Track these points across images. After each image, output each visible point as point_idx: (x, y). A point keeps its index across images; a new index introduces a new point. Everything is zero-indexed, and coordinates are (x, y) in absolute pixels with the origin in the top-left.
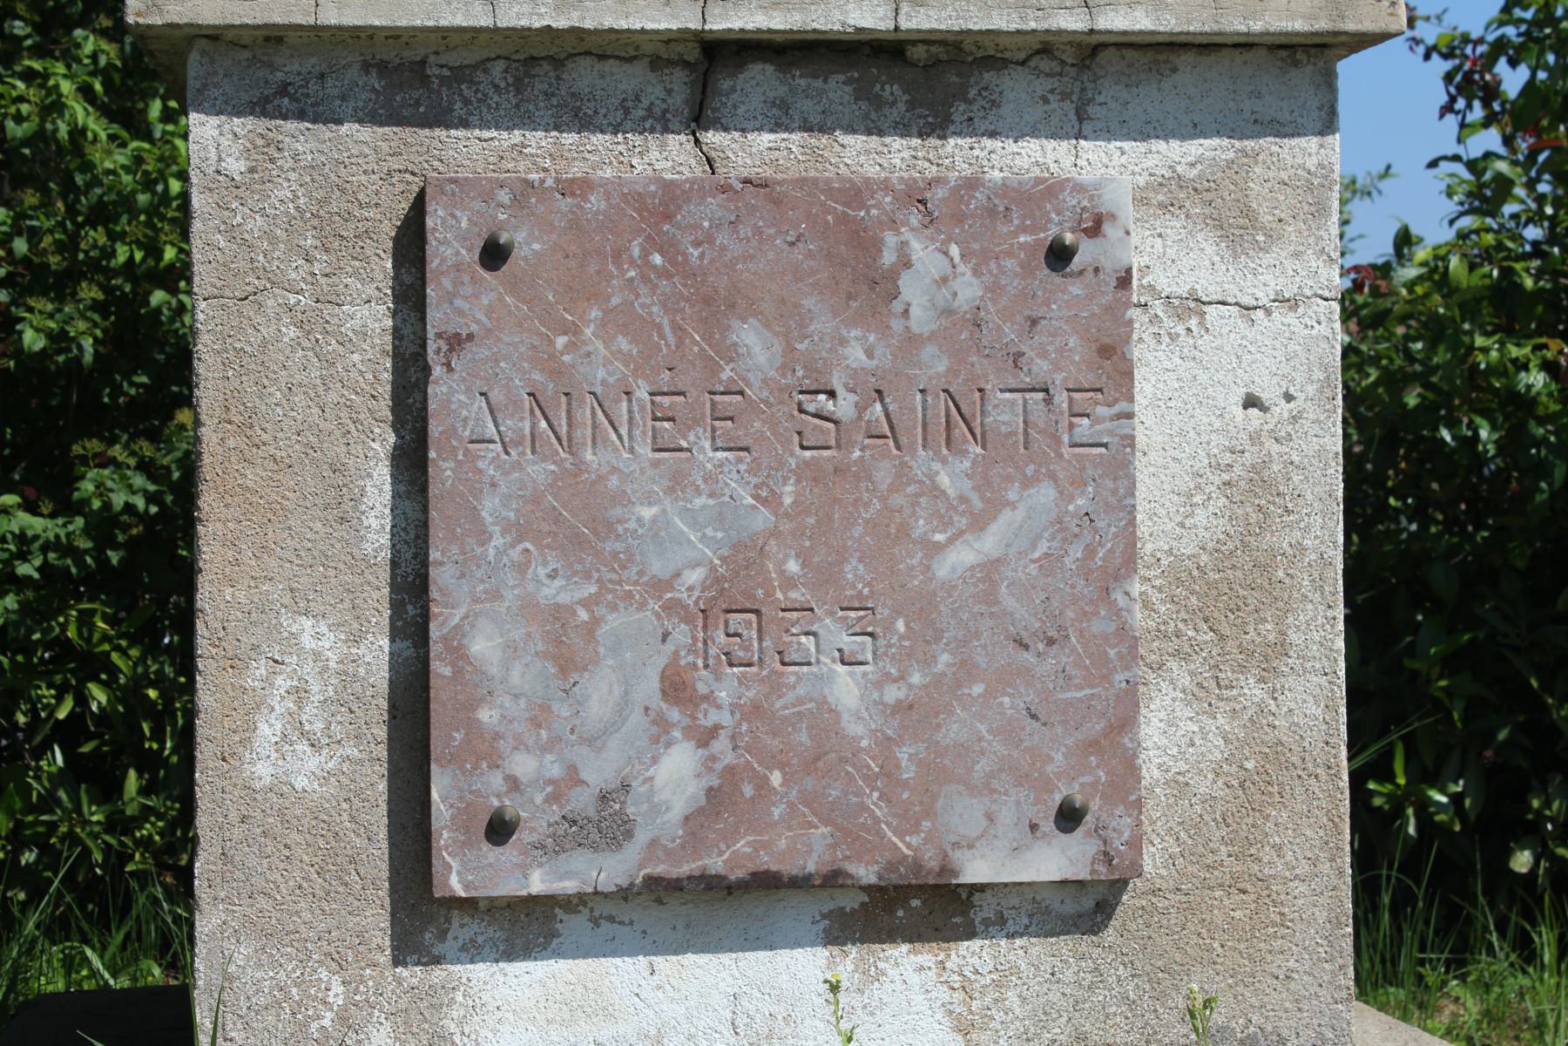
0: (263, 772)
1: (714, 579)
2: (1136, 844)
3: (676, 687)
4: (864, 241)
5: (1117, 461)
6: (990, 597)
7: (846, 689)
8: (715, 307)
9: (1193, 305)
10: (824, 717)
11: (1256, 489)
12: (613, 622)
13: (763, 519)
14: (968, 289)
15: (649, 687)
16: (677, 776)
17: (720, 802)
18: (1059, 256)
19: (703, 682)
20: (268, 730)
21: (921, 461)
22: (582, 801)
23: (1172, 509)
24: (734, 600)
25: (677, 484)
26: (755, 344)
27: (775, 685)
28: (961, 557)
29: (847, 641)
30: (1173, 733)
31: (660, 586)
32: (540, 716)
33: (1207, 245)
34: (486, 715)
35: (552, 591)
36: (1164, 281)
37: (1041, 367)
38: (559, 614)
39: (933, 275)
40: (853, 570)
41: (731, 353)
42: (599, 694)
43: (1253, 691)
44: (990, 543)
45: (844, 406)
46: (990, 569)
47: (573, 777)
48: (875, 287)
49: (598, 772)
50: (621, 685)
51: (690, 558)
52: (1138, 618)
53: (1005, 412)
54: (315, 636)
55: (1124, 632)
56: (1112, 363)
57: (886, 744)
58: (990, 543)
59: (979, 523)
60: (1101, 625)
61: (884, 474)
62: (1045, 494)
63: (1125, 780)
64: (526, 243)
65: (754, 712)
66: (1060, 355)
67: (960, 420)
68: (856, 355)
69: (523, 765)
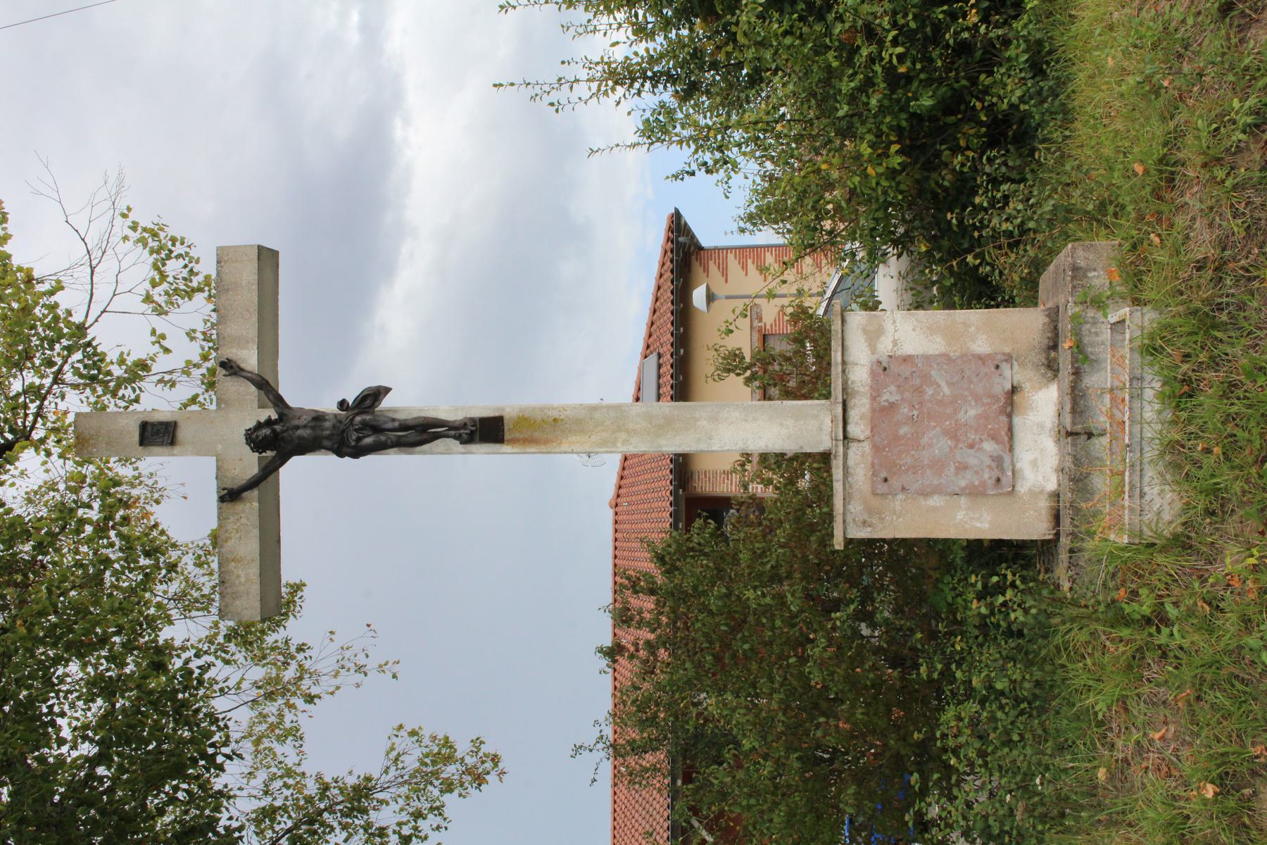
0: (986, 526)
1: (951, 438)
2: (1004, 354)
3: (971, 446)
4: (883, 409)
5: (927, 358)
6: (953, 384)
7: (972, 413)
8: (897, 438)
9: (895, 343)
10: (978, 417)
11: (931, 330)
12: (958, 459)
13: (938, 429)
14: (892, 388)
15: (971, 452)
16: (989, 446)
17: (994, 438)
18: (885, 369)
19: (970, 441)
20: (978, 525)
21: (927, 397)
22: (994, 465)
23: (936, 346)
24: (953, 434)
25: (930, 445)
26: (903, 430)
27: (971, 427)
28: (946, 390)
29: (962, 412)
30: (981, 346)
31: (951, 449)
32: (977, 473)
33: (883, 338)
34: (976, 483)
35: (952, 470)
36: (890, 346)
37: (908, 373)
38: (957, 469)
39: (890, 395)
40: (948, 411)
41: (905, 435)
42: (972, 461)
43: (973, 329)
44: (943, 384)
45: (916, 413)
46: (950, 384)
47: (989, 467)
48: (892, 406)
49: (988, 461)
50: (972, 459)
51: (946, 443)
52: (958, 354)
53: (917, 382)
54: (960, 516)
55: (961, 357)
56: (907, 359)
57: (984, 405)
58: (943, 384)
59: (939, 386)
60: (959, 362)
61: (929, 405)
62: (933, 373)
63: (990, 356)
64: (884, 475)
65: (976, 431)
66: (906, 370)
67: (919, 390)
68: (906, 410)
69: (986, 476)
